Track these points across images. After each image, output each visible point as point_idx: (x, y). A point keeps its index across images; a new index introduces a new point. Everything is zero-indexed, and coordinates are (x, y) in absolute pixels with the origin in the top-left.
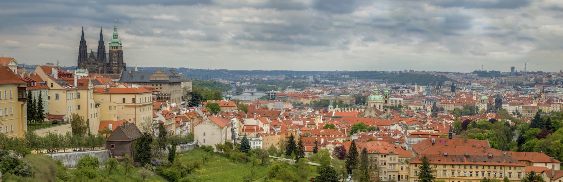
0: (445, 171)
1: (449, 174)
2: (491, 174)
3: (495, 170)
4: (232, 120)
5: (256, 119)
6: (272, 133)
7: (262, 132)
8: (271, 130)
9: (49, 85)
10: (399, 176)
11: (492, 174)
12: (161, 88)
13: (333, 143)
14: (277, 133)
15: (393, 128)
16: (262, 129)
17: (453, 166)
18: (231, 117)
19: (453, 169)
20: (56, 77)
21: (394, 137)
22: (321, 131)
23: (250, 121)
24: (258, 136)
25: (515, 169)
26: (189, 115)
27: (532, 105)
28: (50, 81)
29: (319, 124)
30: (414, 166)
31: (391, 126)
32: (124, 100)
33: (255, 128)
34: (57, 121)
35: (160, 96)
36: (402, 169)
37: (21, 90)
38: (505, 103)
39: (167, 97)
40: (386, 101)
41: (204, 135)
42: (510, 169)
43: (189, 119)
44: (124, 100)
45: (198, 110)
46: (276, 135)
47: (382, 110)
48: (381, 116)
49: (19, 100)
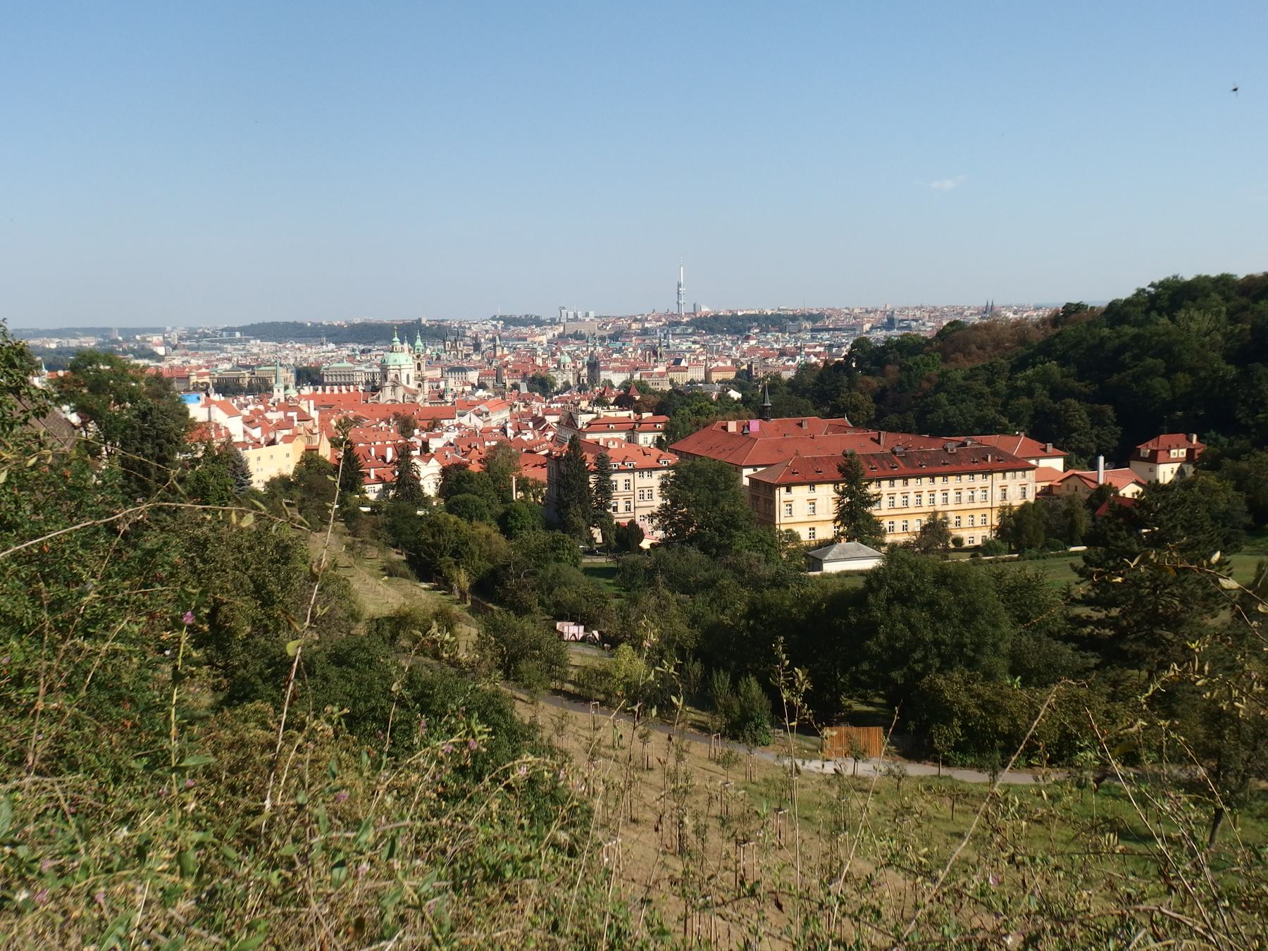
0: (812, 502)
27: (656, 370)
30: (783, 490)
38: (606, 369)
40: (419, 365)
42: (1004, 477)
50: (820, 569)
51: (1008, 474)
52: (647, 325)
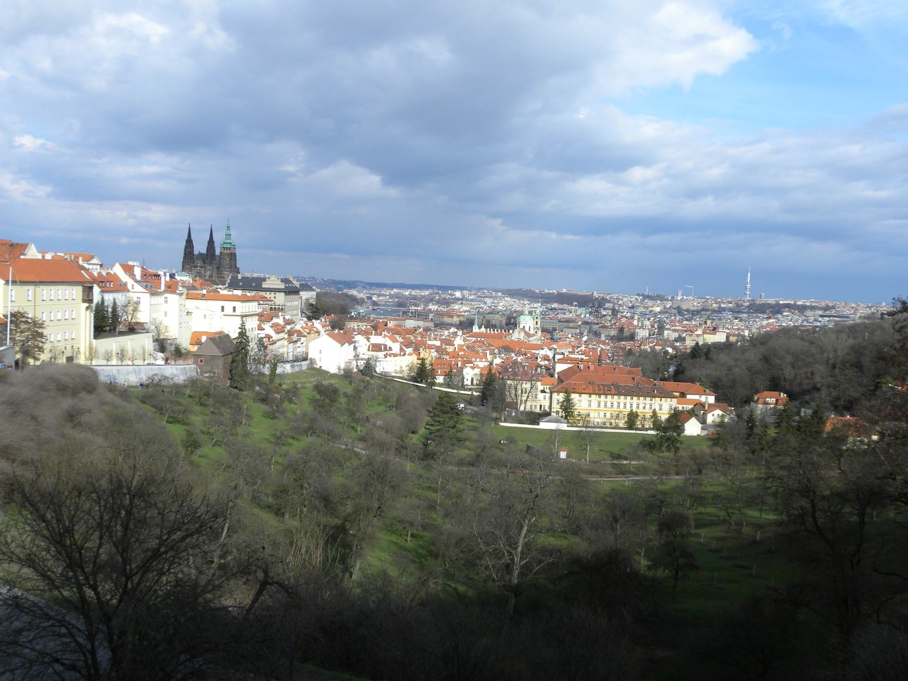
0: (590, 402)
1: (594, 404)
2: (640, 406)
3: (644, 402)
4: (356, 337)
5: (384, 337)
6: (402, 353)
7: (391, 352)
8: (401, 349)
9: (129, 287)
10: (541, 406)
11: (641, 406)
12: (275, 298)
13: (471, 367)
14: (407, 353)
15: (542, 353)
16: (390, 349)
17: (600, 395)
18: (355, 333)
19: (599, 399)
20: (138, 277)
21: (541, 363)
22: (460, 354)
23: (376, 339)
24: (385, 356)
25: (666, 401)
26: (306, 330)
27: (696, 333)
28: (130, 282)
29: (458, 345)
31: (541, 350)
32: (223, 308)
33: (383, 347)
34: (133, 329)
35: (273, 307)
36: (545, 398)
37: (88, 290)
38: (668, 329)
39: (281, 307)
40: (537, 322)
41: (320, 353)
42: (661, 400)
43: (305, 334)
44: (223, 308)
45: (317, 324)
46: (406, 355)
47: (532, 332)
48: (530, 339)
49: (84, 301)
50: (539, 425)
51: (663, 399)
52: (723, 305)
